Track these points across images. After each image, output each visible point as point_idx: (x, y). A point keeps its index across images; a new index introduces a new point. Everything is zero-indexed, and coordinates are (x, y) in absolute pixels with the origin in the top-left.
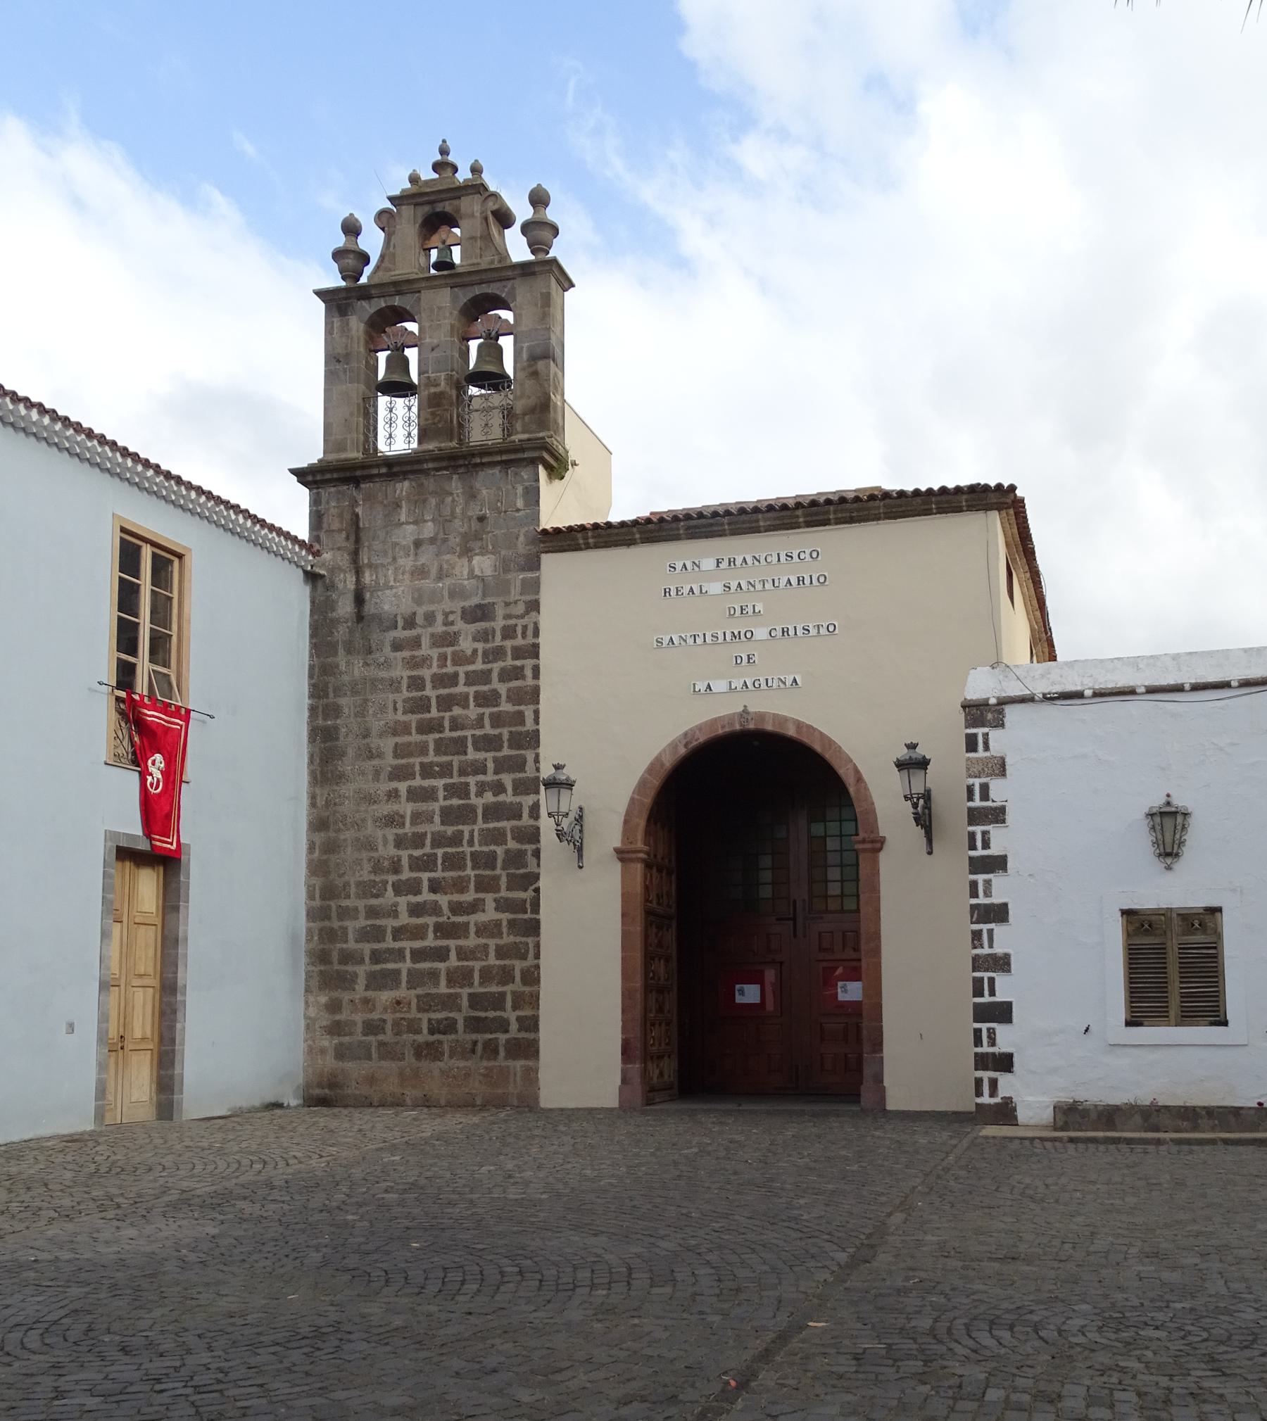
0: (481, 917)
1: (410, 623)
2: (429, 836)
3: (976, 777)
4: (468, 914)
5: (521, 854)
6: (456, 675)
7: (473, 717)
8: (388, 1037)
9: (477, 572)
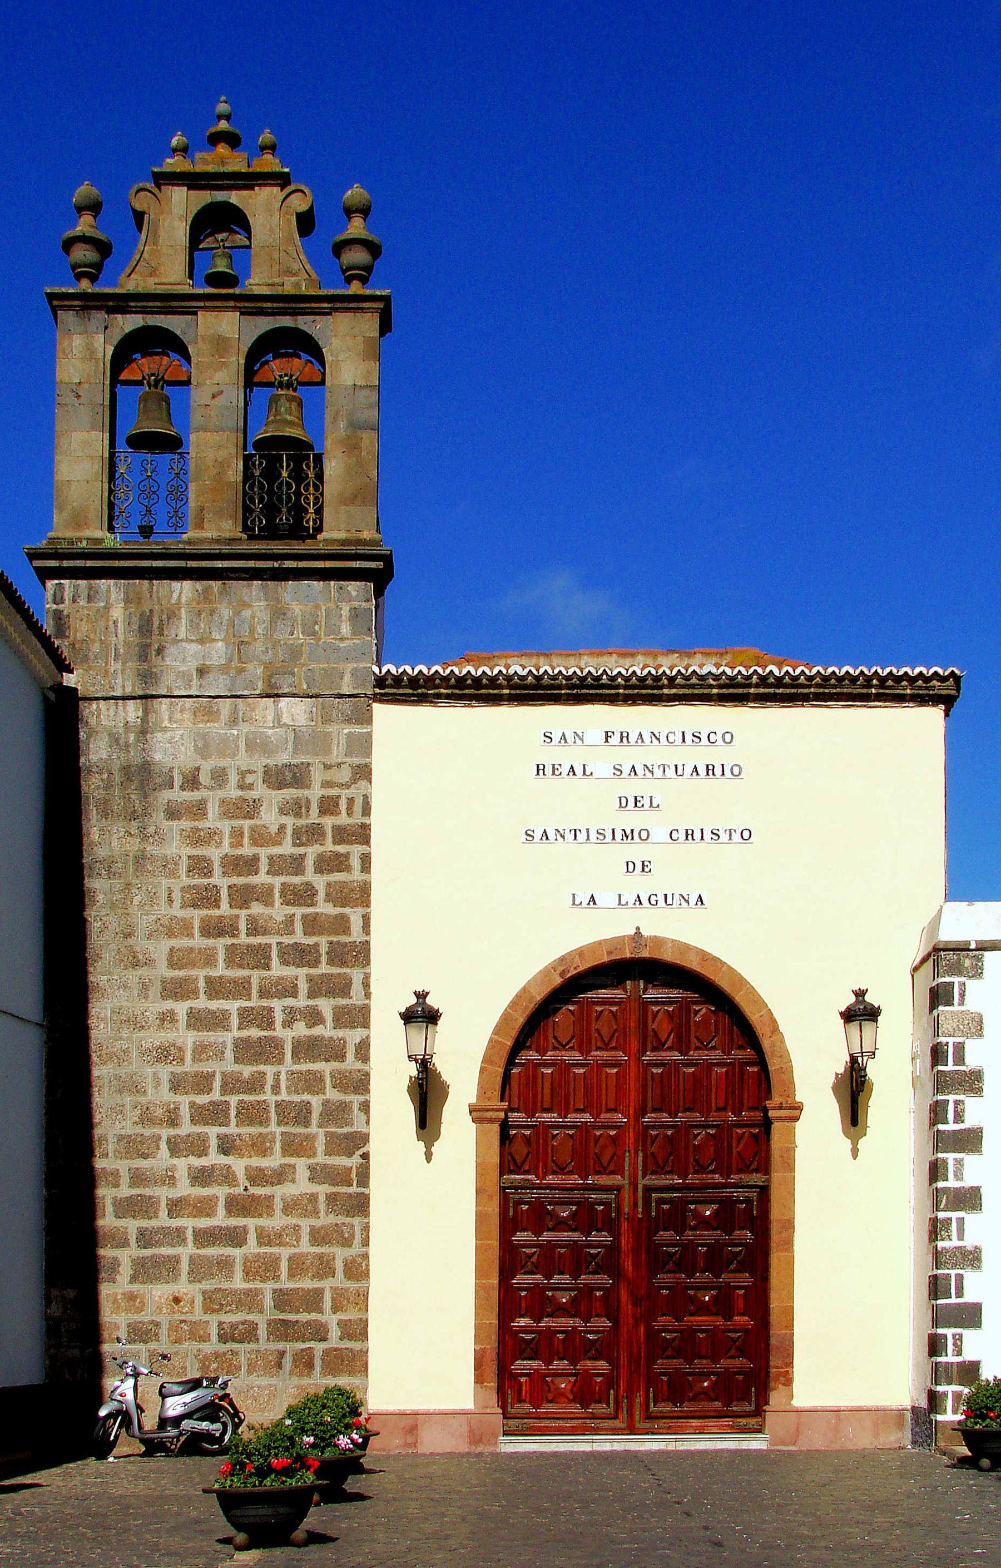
1: (192, 781)
2: (218, 1077)
4: (272, 1184)
5: (344, 1108)
6: (256, 859)
7: (280, 918)
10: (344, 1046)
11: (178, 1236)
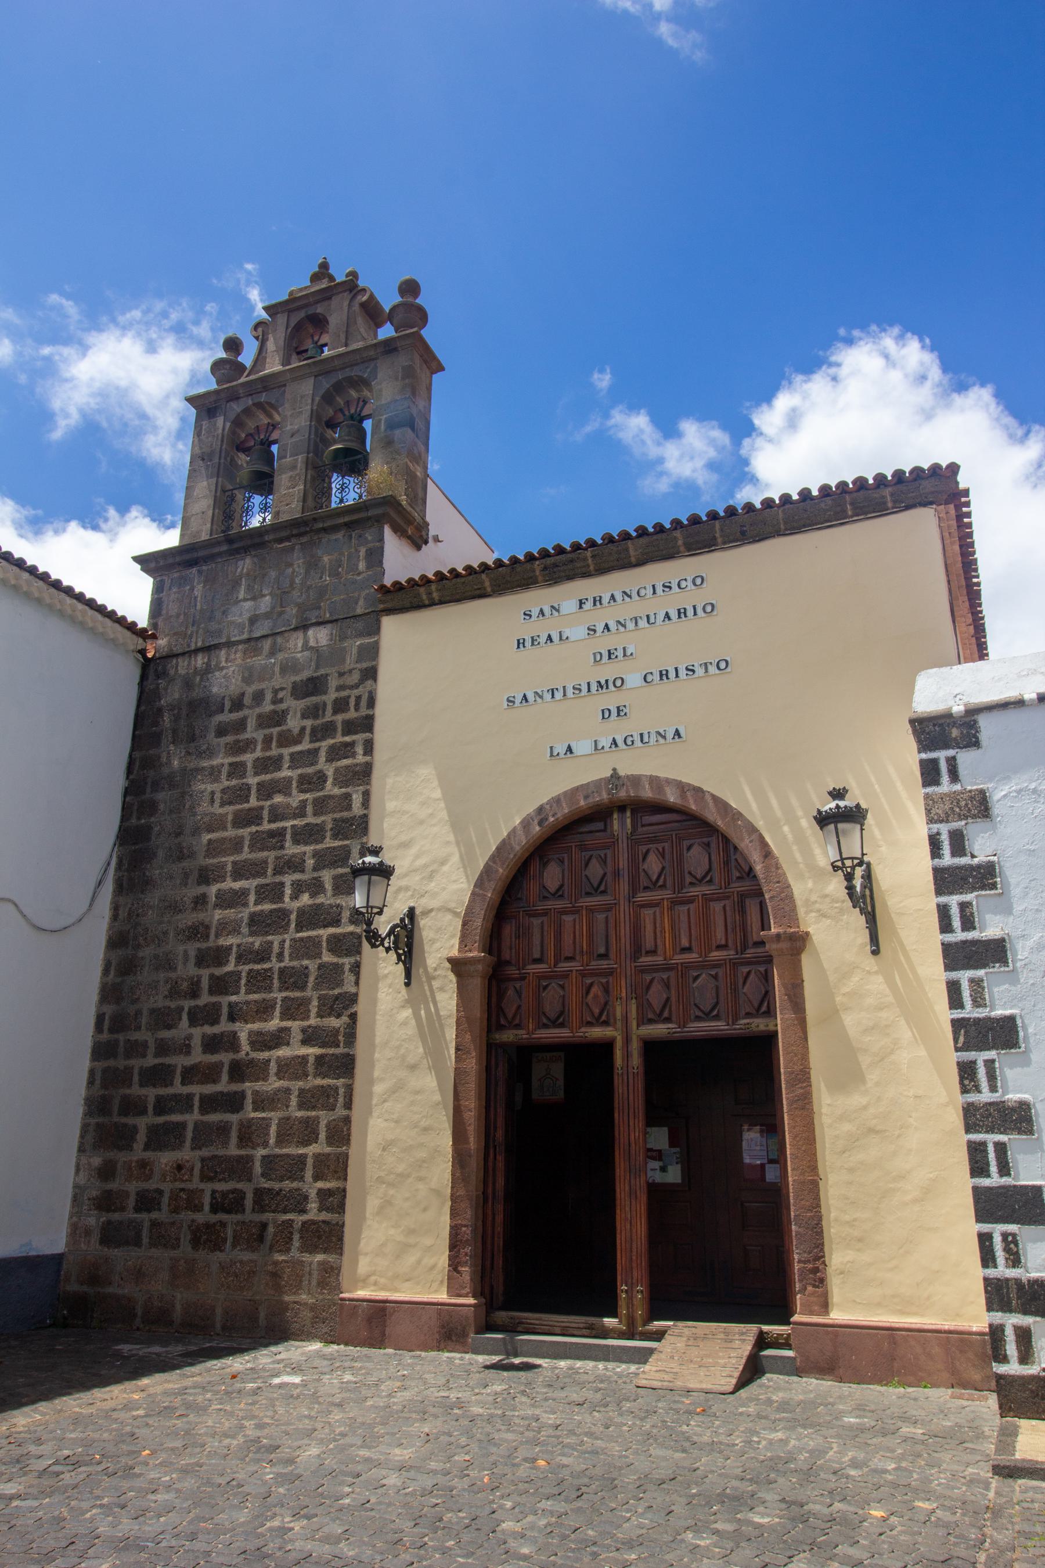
0: (283, 1052)
1: (238, 704)
2: (235, 949)
3: (941, 822)
4: (270, 1048)
5: (338, 968)
6: (281, 757)
7: (295, 805)
8: (162, 1215)
9: (312, 643)
10: (340, 914)
11: (184, 1103)
